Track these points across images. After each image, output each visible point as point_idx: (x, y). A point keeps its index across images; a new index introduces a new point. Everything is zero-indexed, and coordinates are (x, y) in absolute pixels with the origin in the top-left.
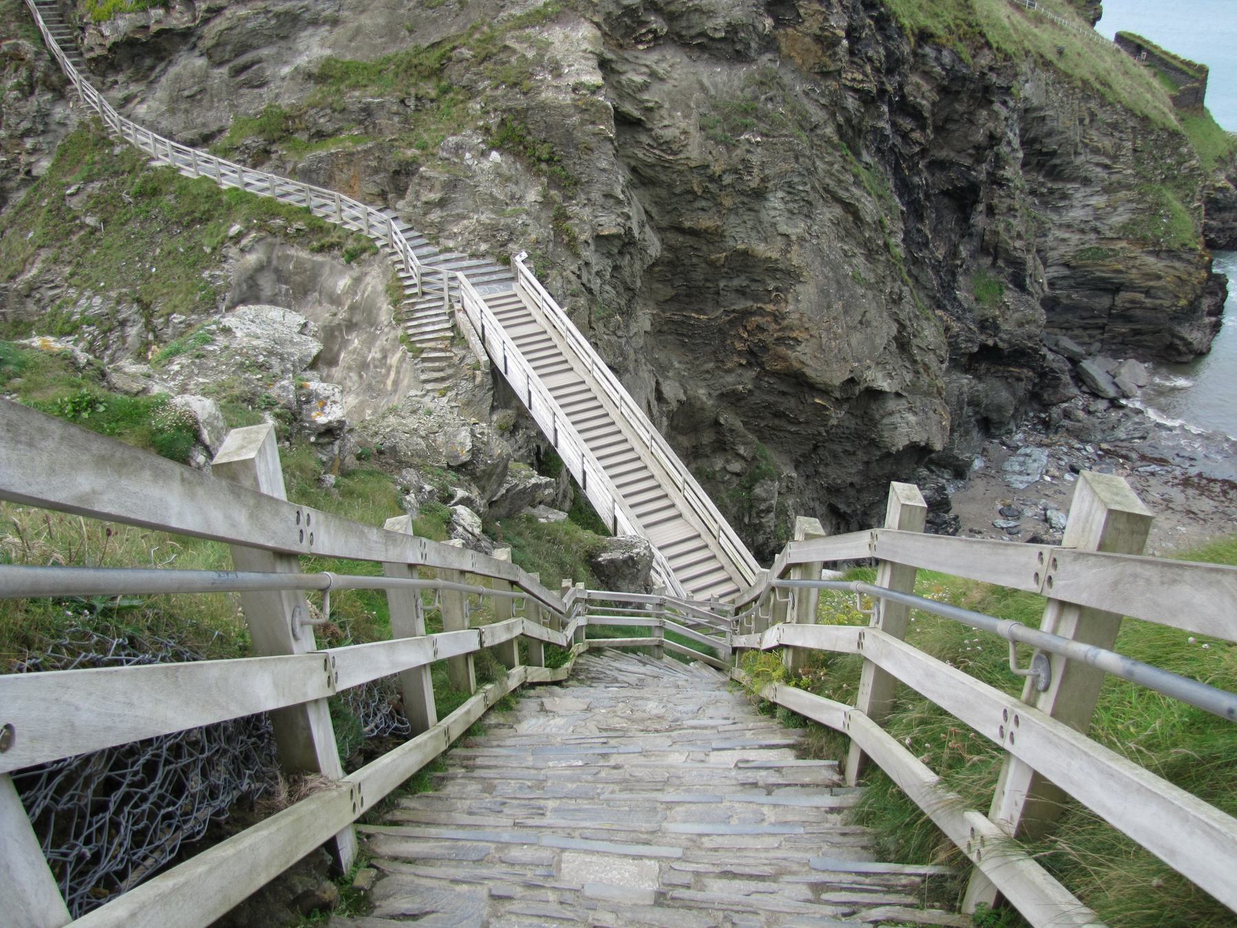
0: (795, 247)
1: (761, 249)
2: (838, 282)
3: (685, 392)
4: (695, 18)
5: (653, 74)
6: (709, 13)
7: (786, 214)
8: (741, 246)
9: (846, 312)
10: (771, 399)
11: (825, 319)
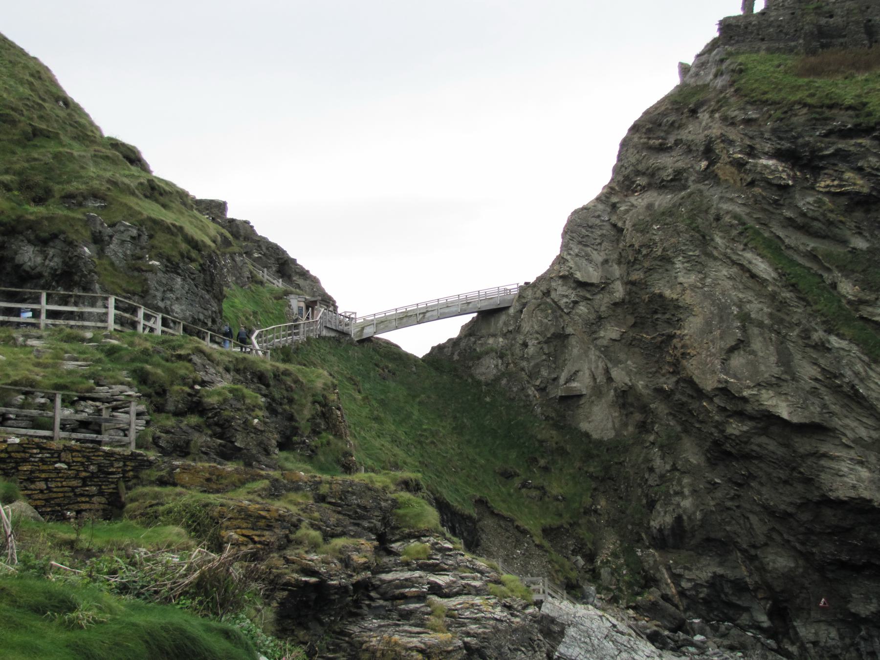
0: (688, 291)
1: (667, 293)
2: (721, 317)
3: (630, 380)
4: (661, 172)
5: (633, 205)
6: (664, 168)
7: (684, 271)
8: (657, 291)
9: (721, 338)
10: (684, 399)
11: (705, 341)
